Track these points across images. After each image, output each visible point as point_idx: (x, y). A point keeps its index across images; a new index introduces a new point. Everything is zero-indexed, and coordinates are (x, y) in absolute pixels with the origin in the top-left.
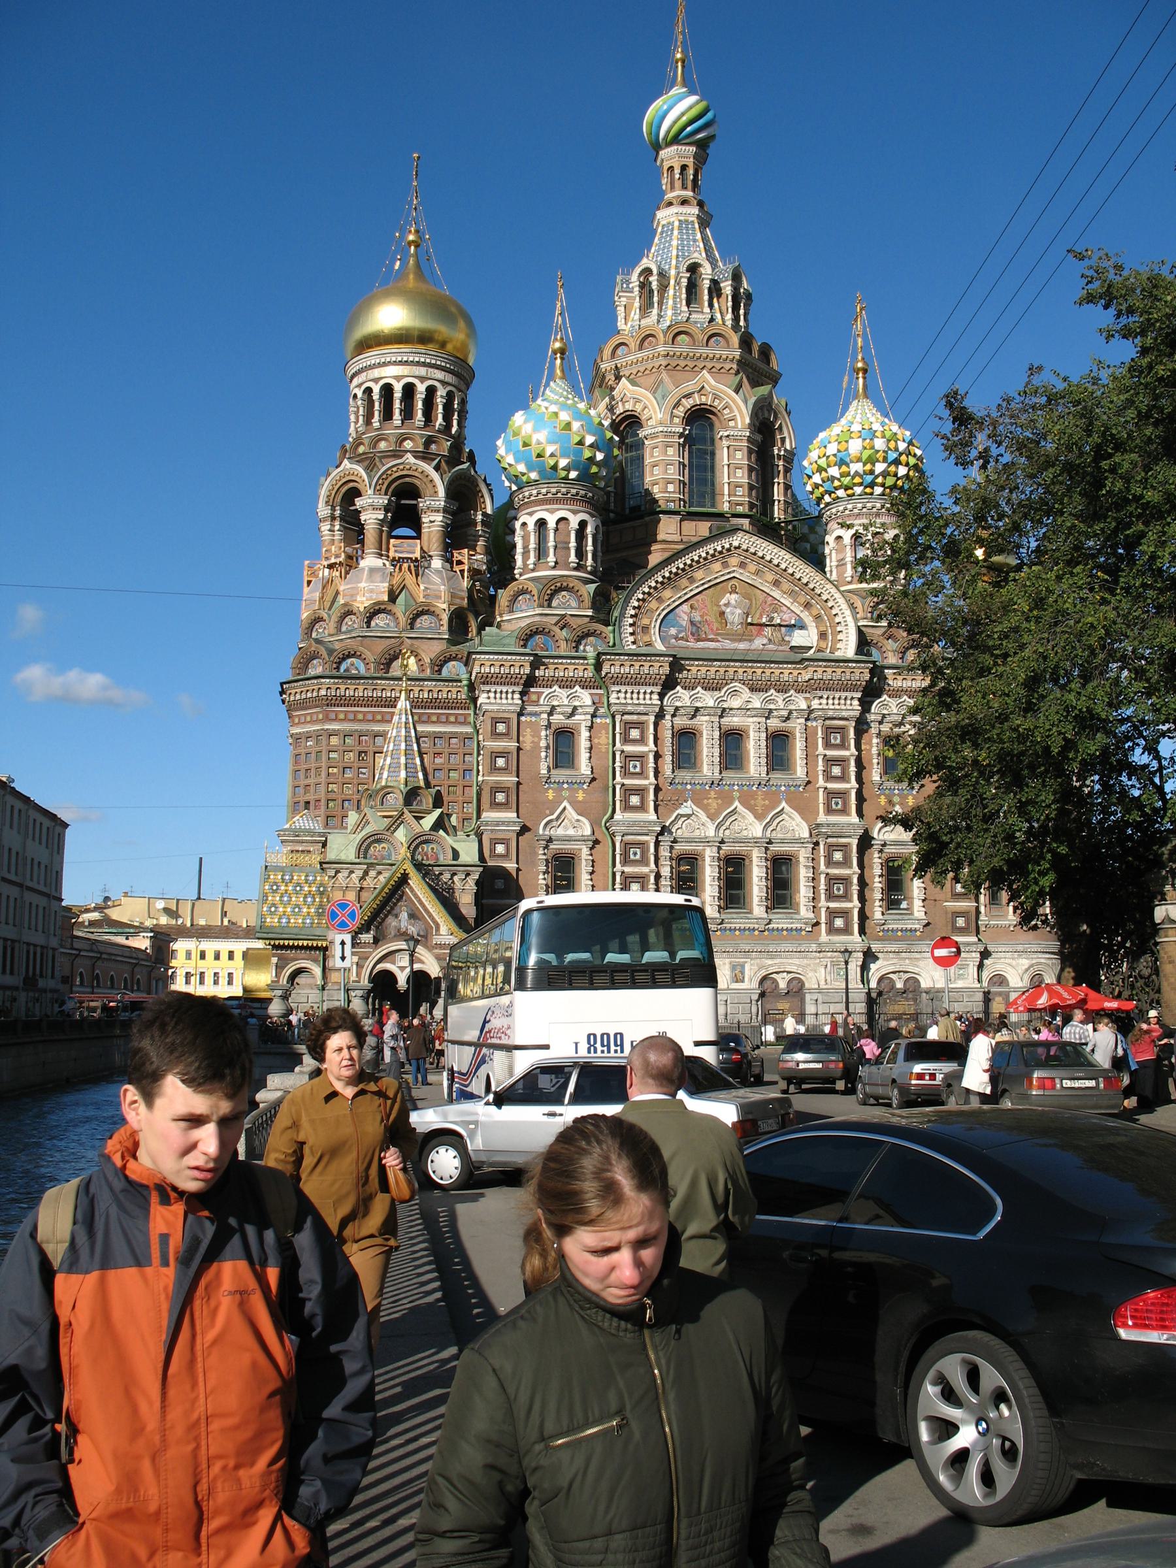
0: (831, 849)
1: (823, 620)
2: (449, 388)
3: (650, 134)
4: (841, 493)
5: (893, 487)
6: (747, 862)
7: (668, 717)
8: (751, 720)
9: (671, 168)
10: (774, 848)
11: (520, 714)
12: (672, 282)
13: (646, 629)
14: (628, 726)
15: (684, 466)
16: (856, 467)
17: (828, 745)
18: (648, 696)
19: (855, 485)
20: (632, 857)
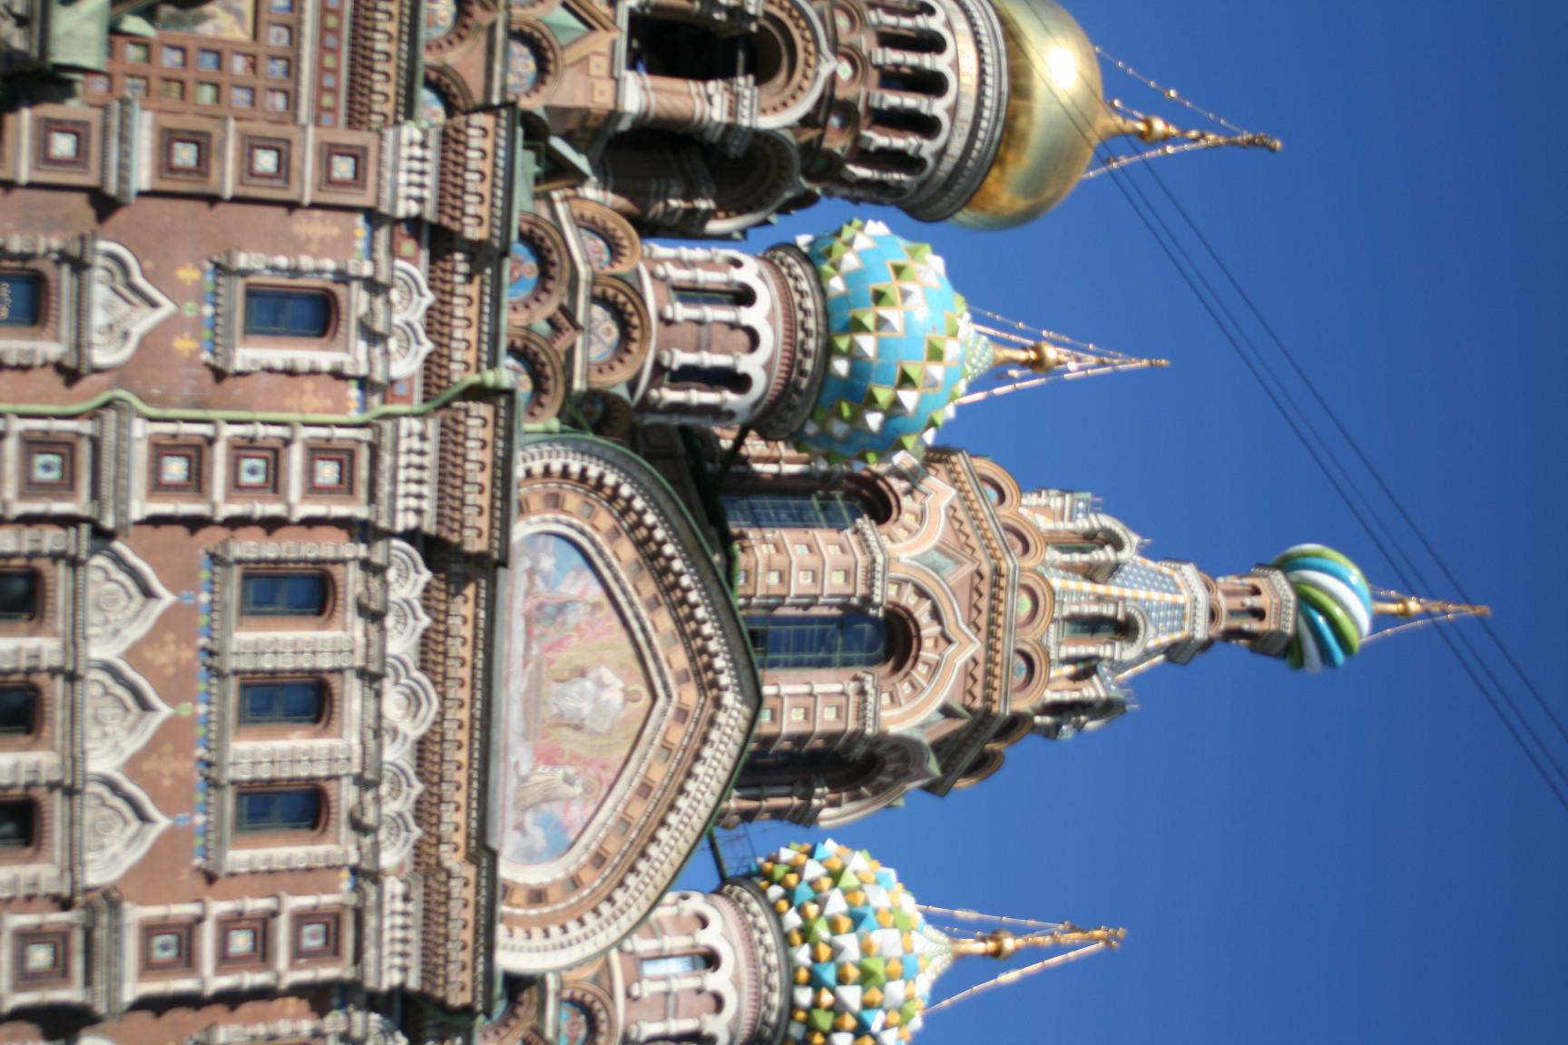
0: (58, 940)
1: (568, 893)
2: (931, 162)
3: (1304, 555)
4: (792, 919)
5: (811, 1027)
6: (23, 739)
7: (362, 550)
8: (355, 740)
9: (1256, 591)
10: (56, 807)
11: (374, 217)
12: (1101, 589)
13: (555, 502)
14: (345, 458)
15: (806, 607)
16: (850, 944)
17: (301, 919)
18: (413, 503)
19: (814, 947)
20: (40, 459)
